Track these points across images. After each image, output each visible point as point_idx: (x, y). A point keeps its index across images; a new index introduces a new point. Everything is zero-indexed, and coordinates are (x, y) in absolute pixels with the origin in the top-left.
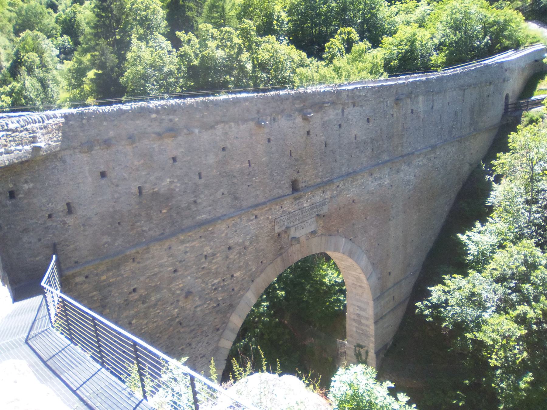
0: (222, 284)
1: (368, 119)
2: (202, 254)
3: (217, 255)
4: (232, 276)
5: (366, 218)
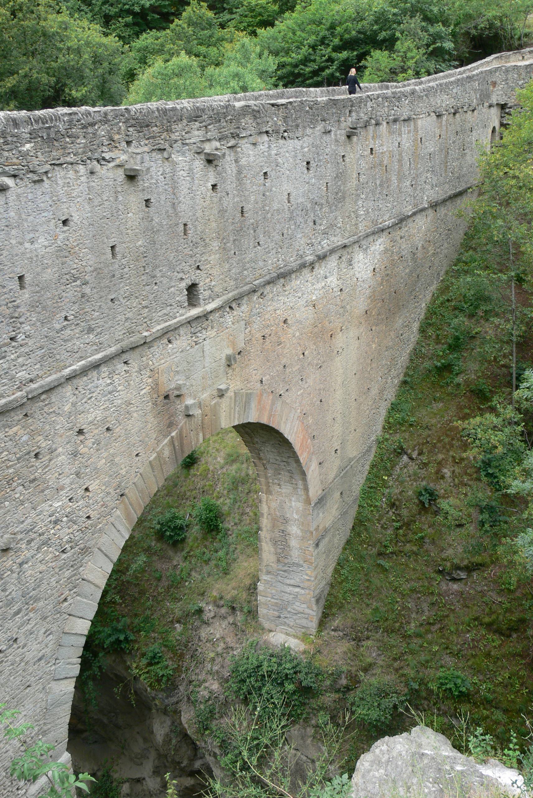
0: (68, 510)
1: (308, 163)
2: (29, 453)
3: (57, 452)
4: (87, 489)
5: (303, 354)
